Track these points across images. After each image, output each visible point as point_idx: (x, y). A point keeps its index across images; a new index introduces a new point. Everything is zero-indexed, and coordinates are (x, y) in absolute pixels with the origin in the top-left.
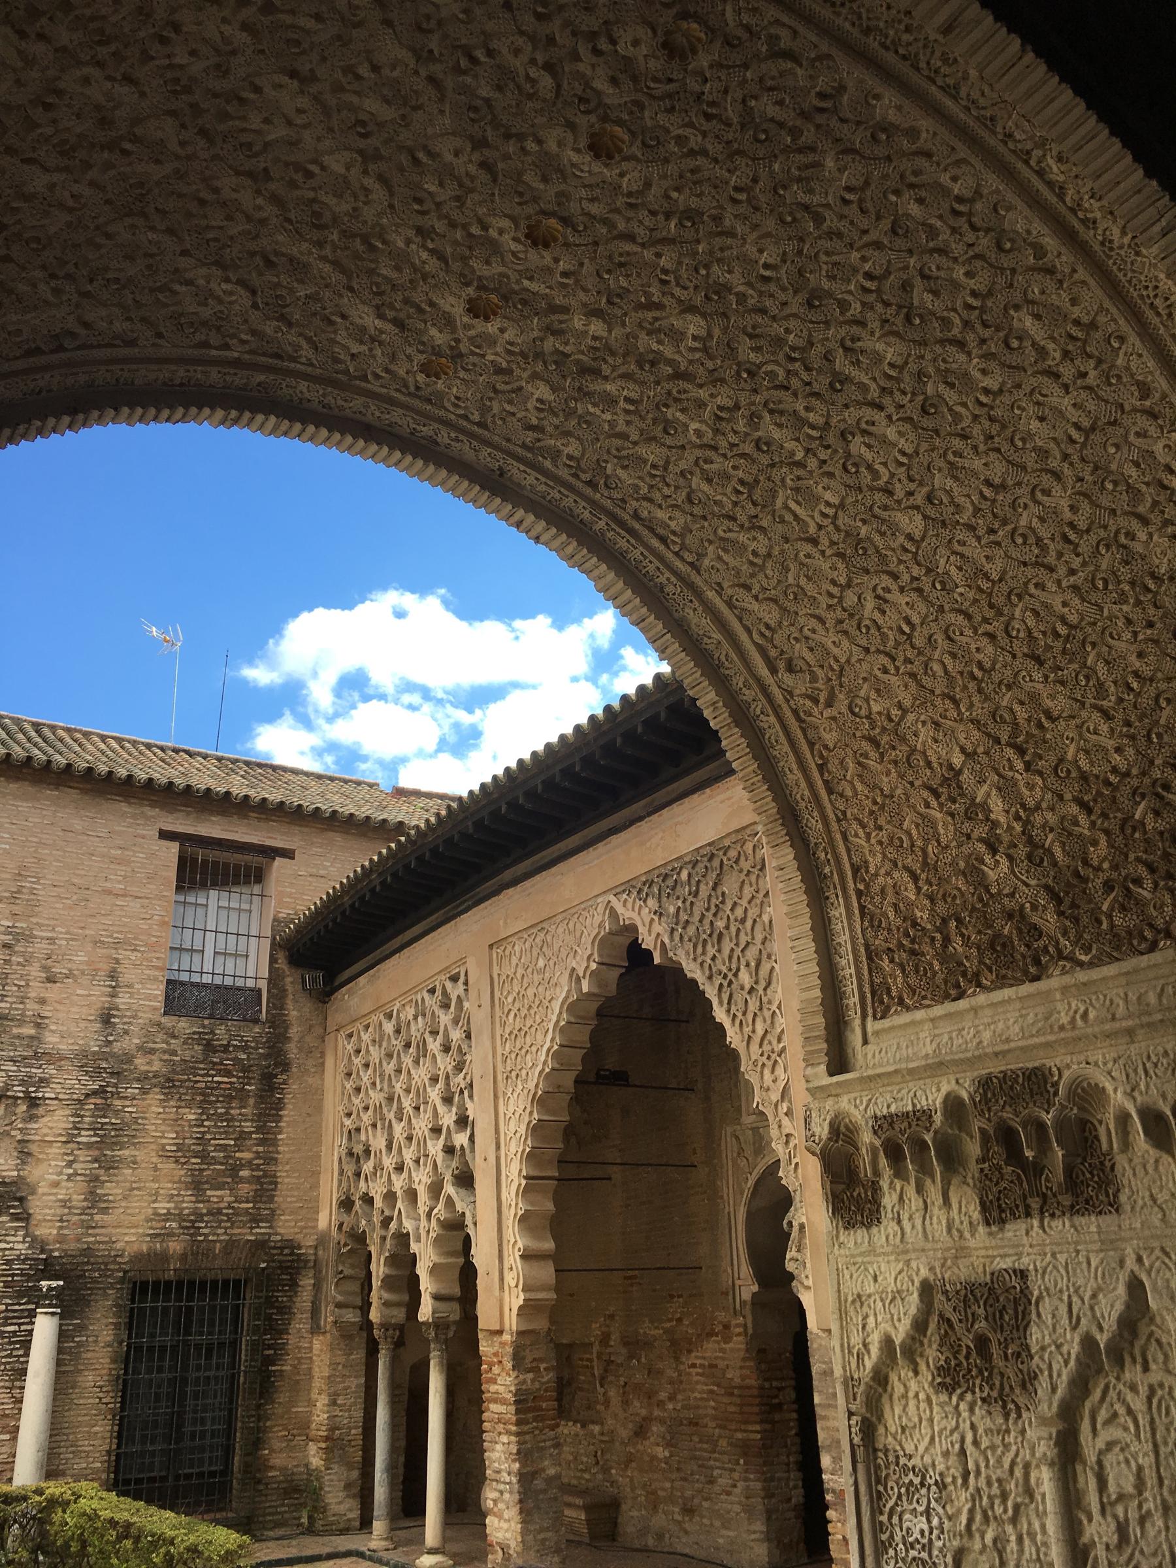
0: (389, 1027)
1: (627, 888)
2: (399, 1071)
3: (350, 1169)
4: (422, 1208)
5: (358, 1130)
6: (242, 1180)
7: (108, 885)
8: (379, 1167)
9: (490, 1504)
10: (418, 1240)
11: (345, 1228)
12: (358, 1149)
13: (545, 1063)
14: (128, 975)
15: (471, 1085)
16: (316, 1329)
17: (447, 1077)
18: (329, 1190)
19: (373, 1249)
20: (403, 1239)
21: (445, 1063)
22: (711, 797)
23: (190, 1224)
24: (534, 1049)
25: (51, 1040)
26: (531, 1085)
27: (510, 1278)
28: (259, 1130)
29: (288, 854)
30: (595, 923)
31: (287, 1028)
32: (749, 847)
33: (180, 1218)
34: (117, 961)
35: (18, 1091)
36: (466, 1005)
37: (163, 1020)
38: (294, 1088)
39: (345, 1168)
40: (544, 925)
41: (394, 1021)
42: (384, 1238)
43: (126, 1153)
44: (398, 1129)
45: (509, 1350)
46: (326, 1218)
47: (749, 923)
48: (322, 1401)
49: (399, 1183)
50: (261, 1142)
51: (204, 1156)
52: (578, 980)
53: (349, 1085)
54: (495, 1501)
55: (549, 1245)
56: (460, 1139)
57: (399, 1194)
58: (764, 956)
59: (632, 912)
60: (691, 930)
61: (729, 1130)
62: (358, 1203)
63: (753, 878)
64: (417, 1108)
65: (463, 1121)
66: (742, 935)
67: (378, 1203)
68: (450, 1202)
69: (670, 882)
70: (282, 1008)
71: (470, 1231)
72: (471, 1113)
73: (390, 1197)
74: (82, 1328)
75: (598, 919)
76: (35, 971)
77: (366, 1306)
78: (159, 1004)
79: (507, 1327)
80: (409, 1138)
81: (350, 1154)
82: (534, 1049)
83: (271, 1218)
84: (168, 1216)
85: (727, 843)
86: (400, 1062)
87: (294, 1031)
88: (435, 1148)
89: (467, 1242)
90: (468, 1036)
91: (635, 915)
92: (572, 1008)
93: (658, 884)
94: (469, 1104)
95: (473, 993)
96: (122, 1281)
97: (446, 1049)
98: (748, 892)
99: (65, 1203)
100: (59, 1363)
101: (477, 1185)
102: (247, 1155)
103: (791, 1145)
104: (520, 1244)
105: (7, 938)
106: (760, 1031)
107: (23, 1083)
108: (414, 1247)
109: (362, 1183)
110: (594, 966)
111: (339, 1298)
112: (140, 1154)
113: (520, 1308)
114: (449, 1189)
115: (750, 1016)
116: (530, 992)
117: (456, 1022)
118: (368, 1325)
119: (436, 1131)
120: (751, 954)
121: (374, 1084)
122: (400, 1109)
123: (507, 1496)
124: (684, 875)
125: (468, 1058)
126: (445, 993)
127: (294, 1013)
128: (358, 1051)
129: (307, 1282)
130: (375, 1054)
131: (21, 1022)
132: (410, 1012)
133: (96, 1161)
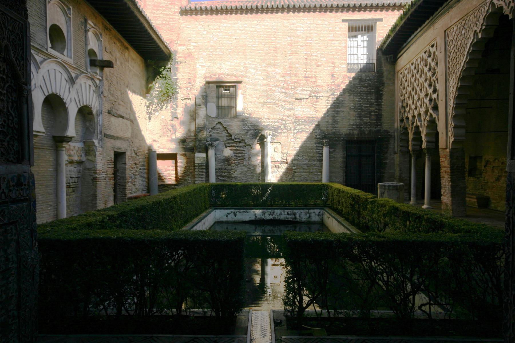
0: (412, 67)
2: (415, 80)
3: (403, 111)
4: (423, 118)
5: (404, 99)
6: (372, 115)
7: (329, 38)
8: (410, 108)
9: (442, 193)
10: (422, 127)
11: (402, 126)
12: (405, 105)
13: (463, 66)
14: (337, 63)
15: (437, 80)
16: (395, 153)
17: (430, 78)
18: (398, 117)
19: (410, 131)
20: (417, 127)
21: (429, 74)
23: (359, 126)
24: (460, 62)
25: (319, 82)
26: (458, 74)
27: (450, 134)
28: (376, 102)
29: (381, 20)
31: (383, 73)
33: (356, 125)
34: (334, 59)
35: (313, 95)
36: (436, 53)
37: (348, 74)
38: (386, 91)
39: (401, 110)
40: (465, 17)
41: (414, 65)
42: (412, 128)
43: (341, 109)
44: (416, 98)
45: (448, 153)
46: (397, 124)
48: (398, 169)
49: (416, 113)
50: (377, 105)
51: (362, 110)
52: (477, 34)
53: (402, 88)
54: (444, 192)
55: (464, 124)
56: (434, 96)
57: (416, 115)
62: (405, 120)
64: (421, 90)
65: (435, 91)
67: (410, 119)
68: (431, 115)
70: (381, 68)
71: (437, 122)
72: (438, 88)
73: (414, 117)
74: (334, 151)
75: (487, 8)
76: (313, 64)
77: (408, 146)
78: (346, 70)
80: (419, 99)
81: (403, 106)
82: (460, 62)
83: (381, 125)
84: (353, 125)
86: (416, 77)
87: (385, 74)
88: (427, 101)
89: (436, 126)
90: (437, 64)
92: (473, 45)
94: (437, 85)
95: (438, 48)
96: (343, 140)
97: (430, 69)
99: (327, 122)
100: (330, 158)
101: (439, 109)
102: (373, 109)
104: (453, 124)
105: (306, 57)
107: (314, 93)
108: (421, 129)
109: (406, 114)
110: (484, 27)
111: (401, 145)
112: (344, 110)
113: (453, 142)
114: (431, 111)
116: (459, 43)
117: (433, 60)
118: (409, 151)
119: (427, 95)
121: (408, 86)
122: (416, 91)
123: (447, 191)
125: (437, 71)
126: (430, 52)
127: (385, 69)
128: (404, 77)
129: (392, 141)
130: (409, 76)
131: (311, 77)
132: (419, 60)
133: (333, 111)
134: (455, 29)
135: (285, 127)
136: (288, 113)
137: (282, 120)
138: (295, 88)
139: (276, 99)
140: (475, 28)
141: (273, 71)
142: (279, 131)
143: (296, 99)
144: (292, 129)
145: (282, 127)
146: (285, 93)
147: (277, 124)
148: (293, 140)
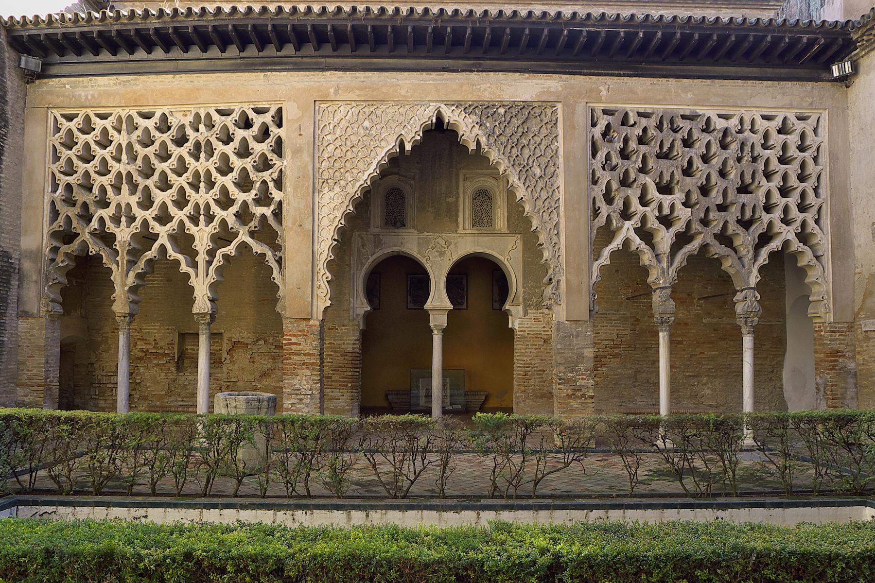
1: (458, 104)
22: (528, 78)
30: (426, 115)
32: (549, 111)
47: (543, 147)
58: (551, 163)
59: (450, 115)
60: (503, 139)
61: (358, 233)
63: (549, 126)
66: (537, 151)
69: (491, 111)
79: (315, 316)
85: (535, 104)
91: (460, 119)
93: (483, 110)
98: (544, 131)
103: (556, 248)
106: (544, 195)
115: (539, 189)
120: (543, 161)
124: (502, 111)
134: (342, 108)
140: (403, 132)
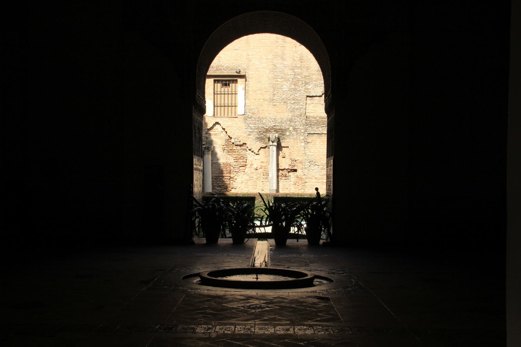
135: (294, 129)
136: (297, 113)
137: (291, 121)
138: (306, 83)
139: (284, 96)
141: (281, 64)
142: (288, 133)
143: (307, 96)
144: (303, 131)
145: (291, 129)
146: (295, 90)
147: (284, 126)
148: (303, 144)
